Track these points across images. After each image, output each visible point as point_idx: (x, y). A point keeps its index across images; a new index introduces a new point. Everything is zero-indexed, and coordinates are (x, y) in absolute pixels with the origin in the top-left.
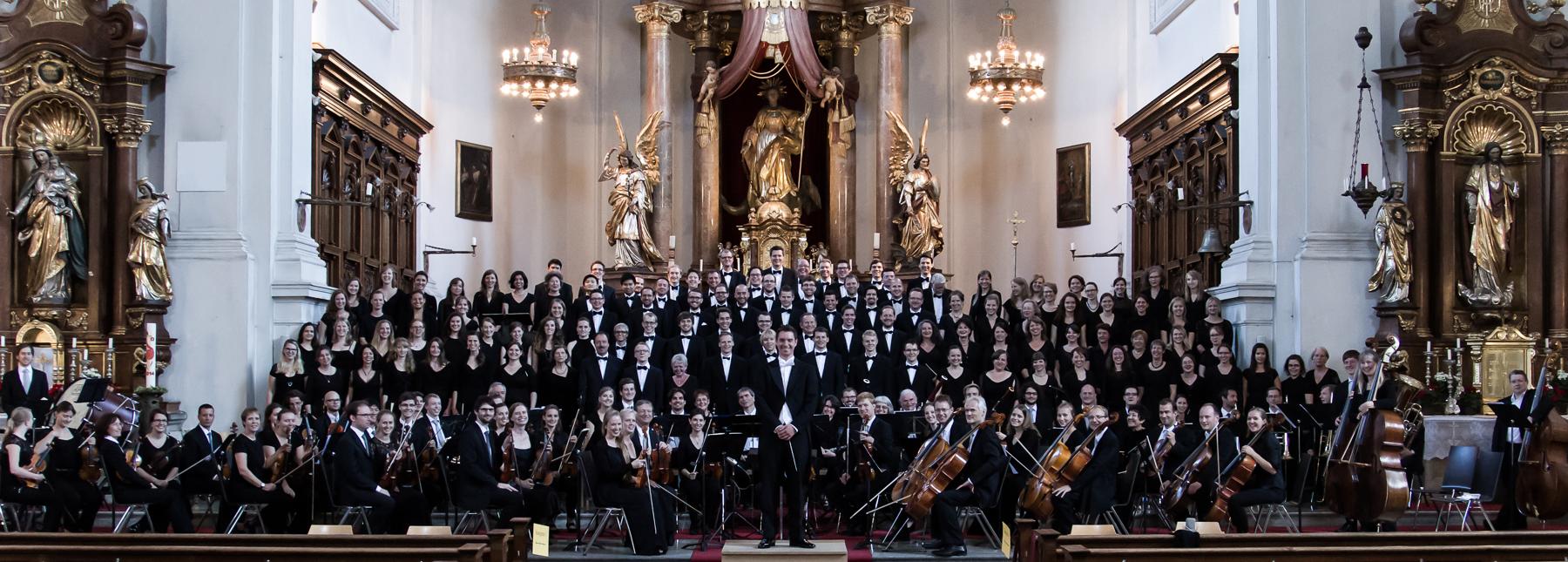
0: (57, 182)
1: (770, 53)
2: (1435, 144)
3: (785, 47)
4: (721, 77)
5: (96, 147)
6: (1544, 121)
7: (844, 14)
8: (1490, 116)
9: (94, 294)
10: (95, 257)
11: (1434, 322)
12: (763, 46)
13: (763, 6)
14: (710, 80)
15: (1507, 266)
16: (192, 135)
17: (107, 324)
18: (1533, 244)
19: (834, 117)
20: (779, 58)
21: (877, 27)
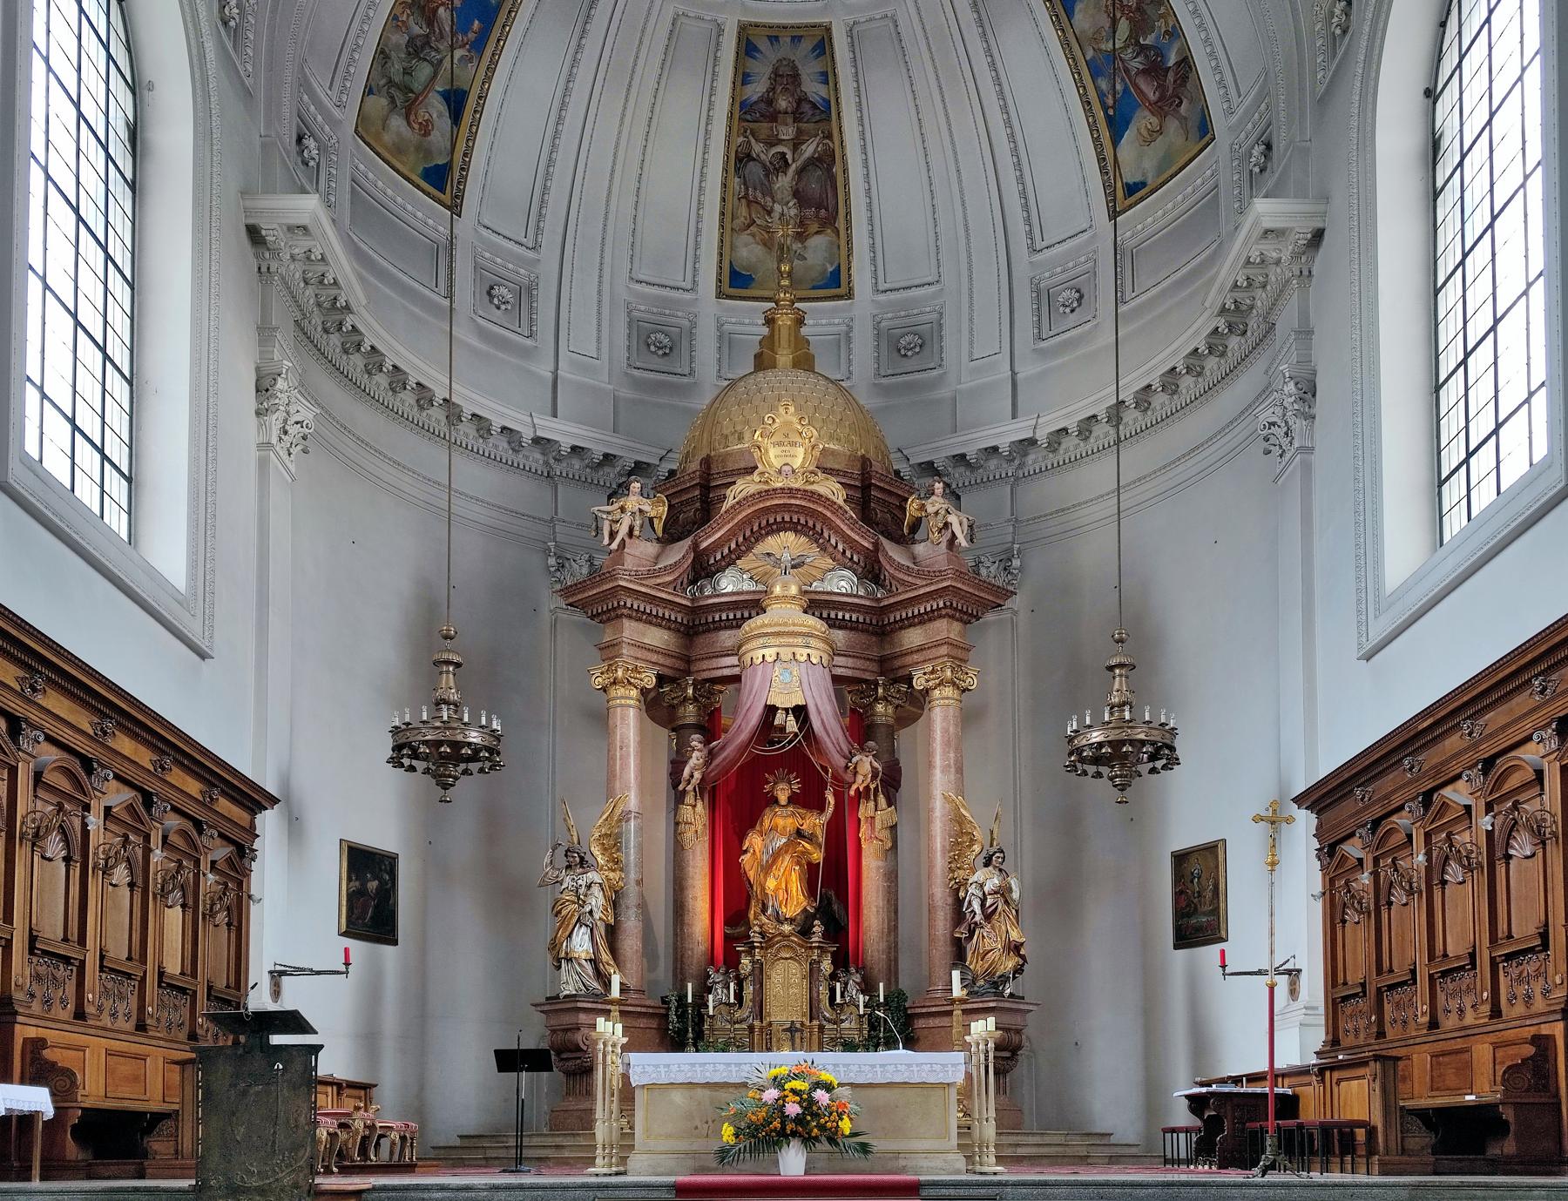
1: (779, 719)
7: (881, 680)
12: (771, 710)
13: (769, 659)
20: (792, 725)
21: (926, 692)
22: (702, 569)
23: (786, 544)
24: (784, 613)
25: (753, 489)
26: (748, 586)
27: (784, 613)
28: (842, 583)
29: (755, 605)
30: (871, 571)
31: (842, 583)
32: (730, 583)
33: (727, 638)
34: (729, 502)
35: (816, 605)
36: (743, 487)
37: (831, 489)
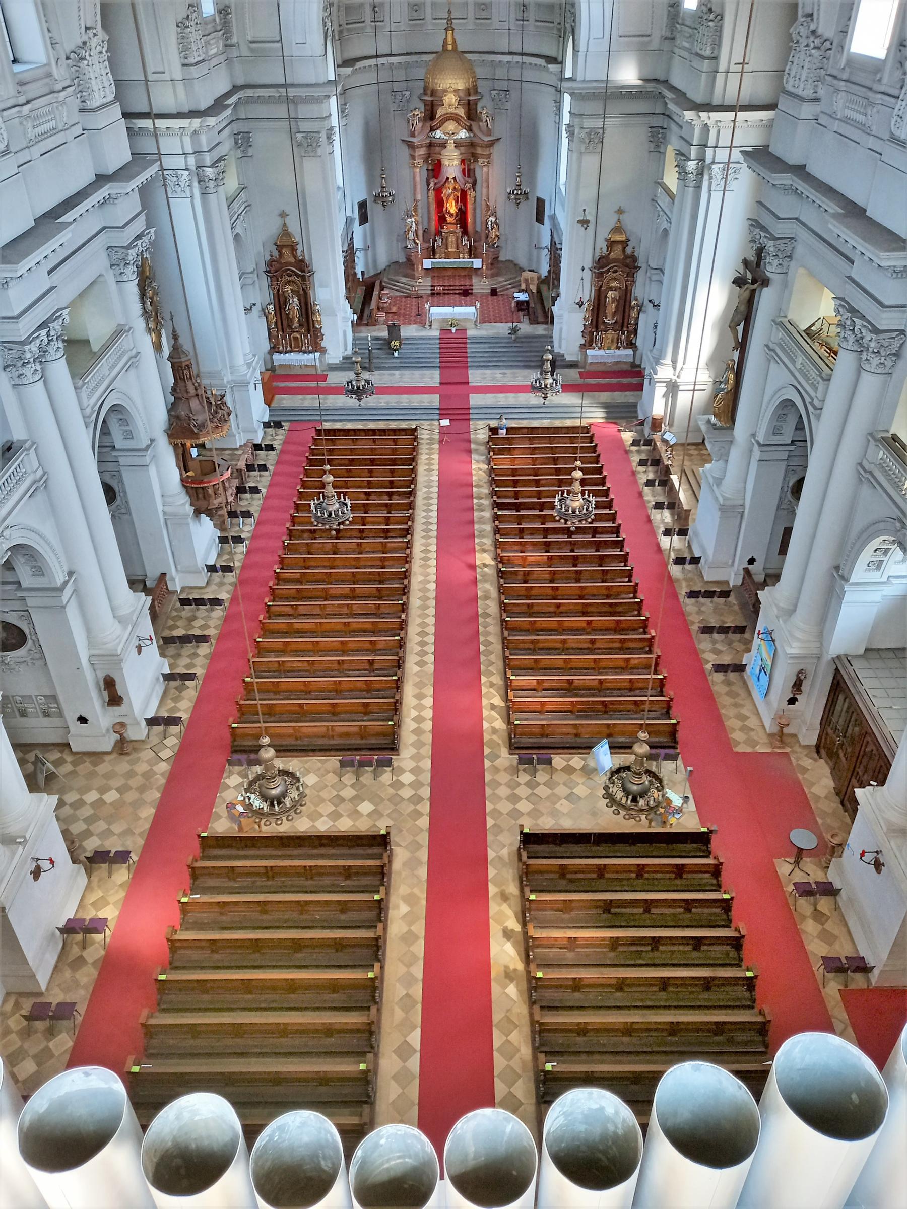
0: (295, 302)
2: (601, 286)
3: (454, 179)
4: (436, 184)
5: (302, 292)
6: (627, 280)
8: (615, 279)
9: (305, 324)
10: (304, 316)
11: (597, 327)
14: (432, 185)
15: (614, 314)
16: (321, 286)
17: (309, 331)
18: (621, 309)
19: (469, 192)
22: (432, 129)
23: (451, 126)
24: (451, 146)
25: (444, 112)
26: (443, 136)
27: (451, 146)
28: (463, 134)
29: (443, 145)
30: (470, 129)
31: (463, 134)
32: (438, 134)
33: (438, 149)
34: (438, 116)
35: (458, 145)
36: (440, 112)
37: (461, 112)
